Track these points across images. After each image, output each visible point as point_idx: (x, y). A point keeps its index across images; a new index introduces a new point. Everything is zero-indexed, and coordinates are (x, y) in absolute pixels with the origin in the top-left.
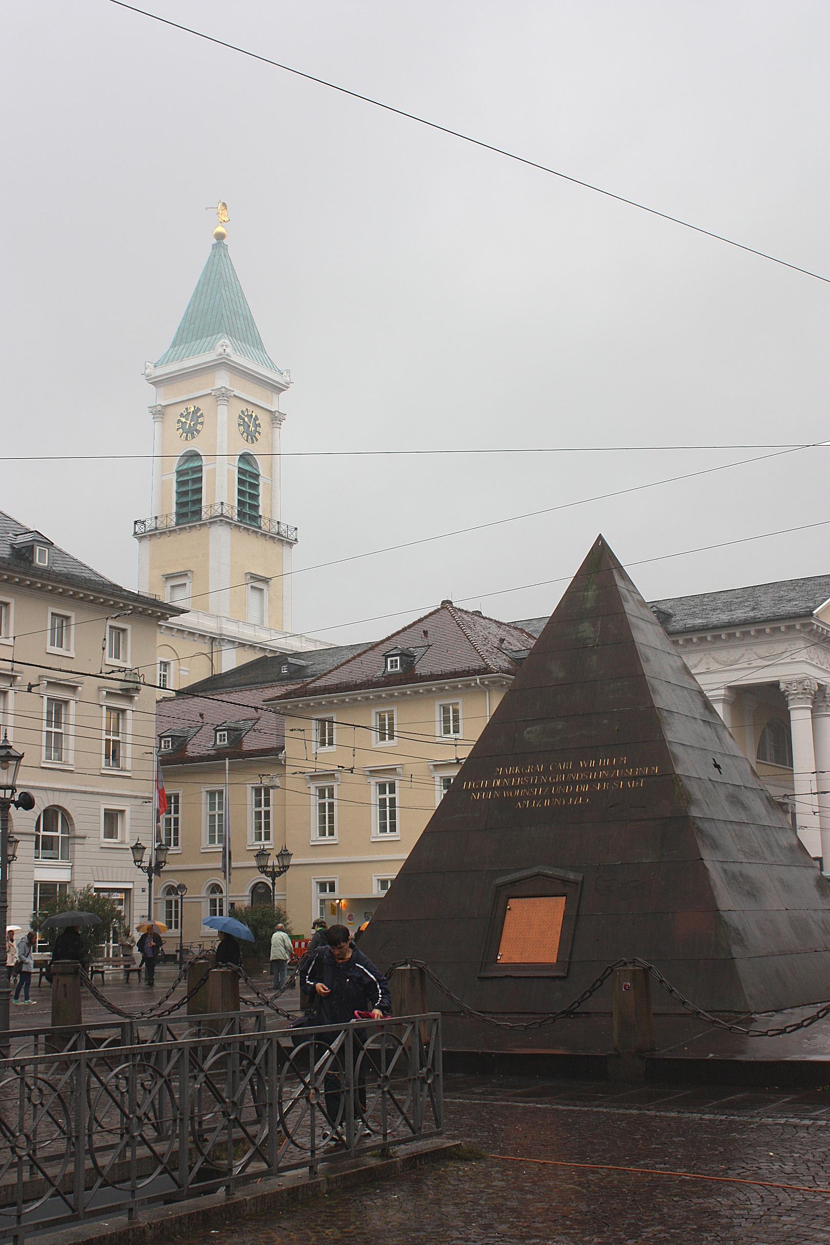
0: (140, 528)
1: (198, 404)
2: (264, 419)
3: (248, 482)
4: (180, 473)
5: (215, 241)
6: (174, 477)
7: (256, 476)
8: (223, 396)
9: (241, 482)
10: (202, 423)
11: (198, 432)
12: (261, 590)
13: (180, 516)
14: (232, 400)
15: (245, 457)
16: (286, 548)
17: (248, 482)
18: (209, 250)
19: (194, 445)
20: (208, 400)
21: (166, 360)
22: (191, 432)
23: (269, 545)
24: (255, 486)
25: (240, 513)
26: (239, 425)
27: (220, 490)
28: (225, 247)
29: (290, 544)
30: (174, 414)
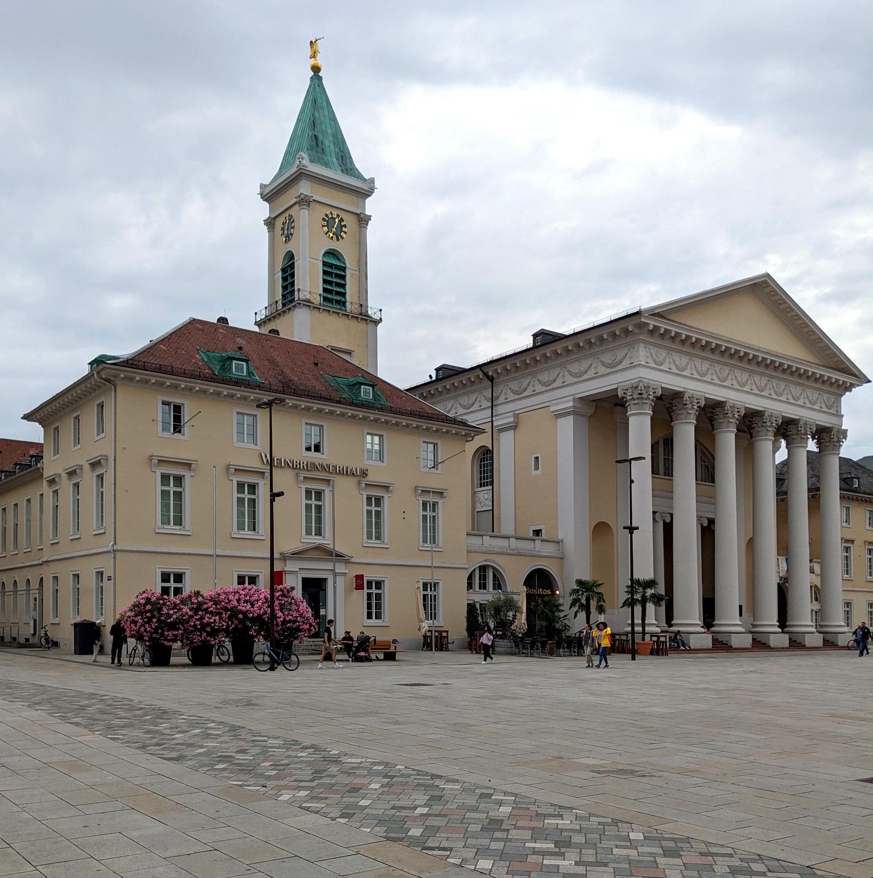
1: (291, 212)
2: (349, 220)
3: (335, 274)
7: (344, 269)
8: (304, 202)
10: (293, 228)
14: (317, 206)
15: (330, 253)
16: (371, 326)
17: (335, 274)
18: (308, 83)
19: (291, 246)
22: (288, 237)
23: (353, 323)
24: (343, 277)
25: (325, 299)
26: (323, 226)
28: (320, 78)
29: (377, 322)
30: (279, 223)
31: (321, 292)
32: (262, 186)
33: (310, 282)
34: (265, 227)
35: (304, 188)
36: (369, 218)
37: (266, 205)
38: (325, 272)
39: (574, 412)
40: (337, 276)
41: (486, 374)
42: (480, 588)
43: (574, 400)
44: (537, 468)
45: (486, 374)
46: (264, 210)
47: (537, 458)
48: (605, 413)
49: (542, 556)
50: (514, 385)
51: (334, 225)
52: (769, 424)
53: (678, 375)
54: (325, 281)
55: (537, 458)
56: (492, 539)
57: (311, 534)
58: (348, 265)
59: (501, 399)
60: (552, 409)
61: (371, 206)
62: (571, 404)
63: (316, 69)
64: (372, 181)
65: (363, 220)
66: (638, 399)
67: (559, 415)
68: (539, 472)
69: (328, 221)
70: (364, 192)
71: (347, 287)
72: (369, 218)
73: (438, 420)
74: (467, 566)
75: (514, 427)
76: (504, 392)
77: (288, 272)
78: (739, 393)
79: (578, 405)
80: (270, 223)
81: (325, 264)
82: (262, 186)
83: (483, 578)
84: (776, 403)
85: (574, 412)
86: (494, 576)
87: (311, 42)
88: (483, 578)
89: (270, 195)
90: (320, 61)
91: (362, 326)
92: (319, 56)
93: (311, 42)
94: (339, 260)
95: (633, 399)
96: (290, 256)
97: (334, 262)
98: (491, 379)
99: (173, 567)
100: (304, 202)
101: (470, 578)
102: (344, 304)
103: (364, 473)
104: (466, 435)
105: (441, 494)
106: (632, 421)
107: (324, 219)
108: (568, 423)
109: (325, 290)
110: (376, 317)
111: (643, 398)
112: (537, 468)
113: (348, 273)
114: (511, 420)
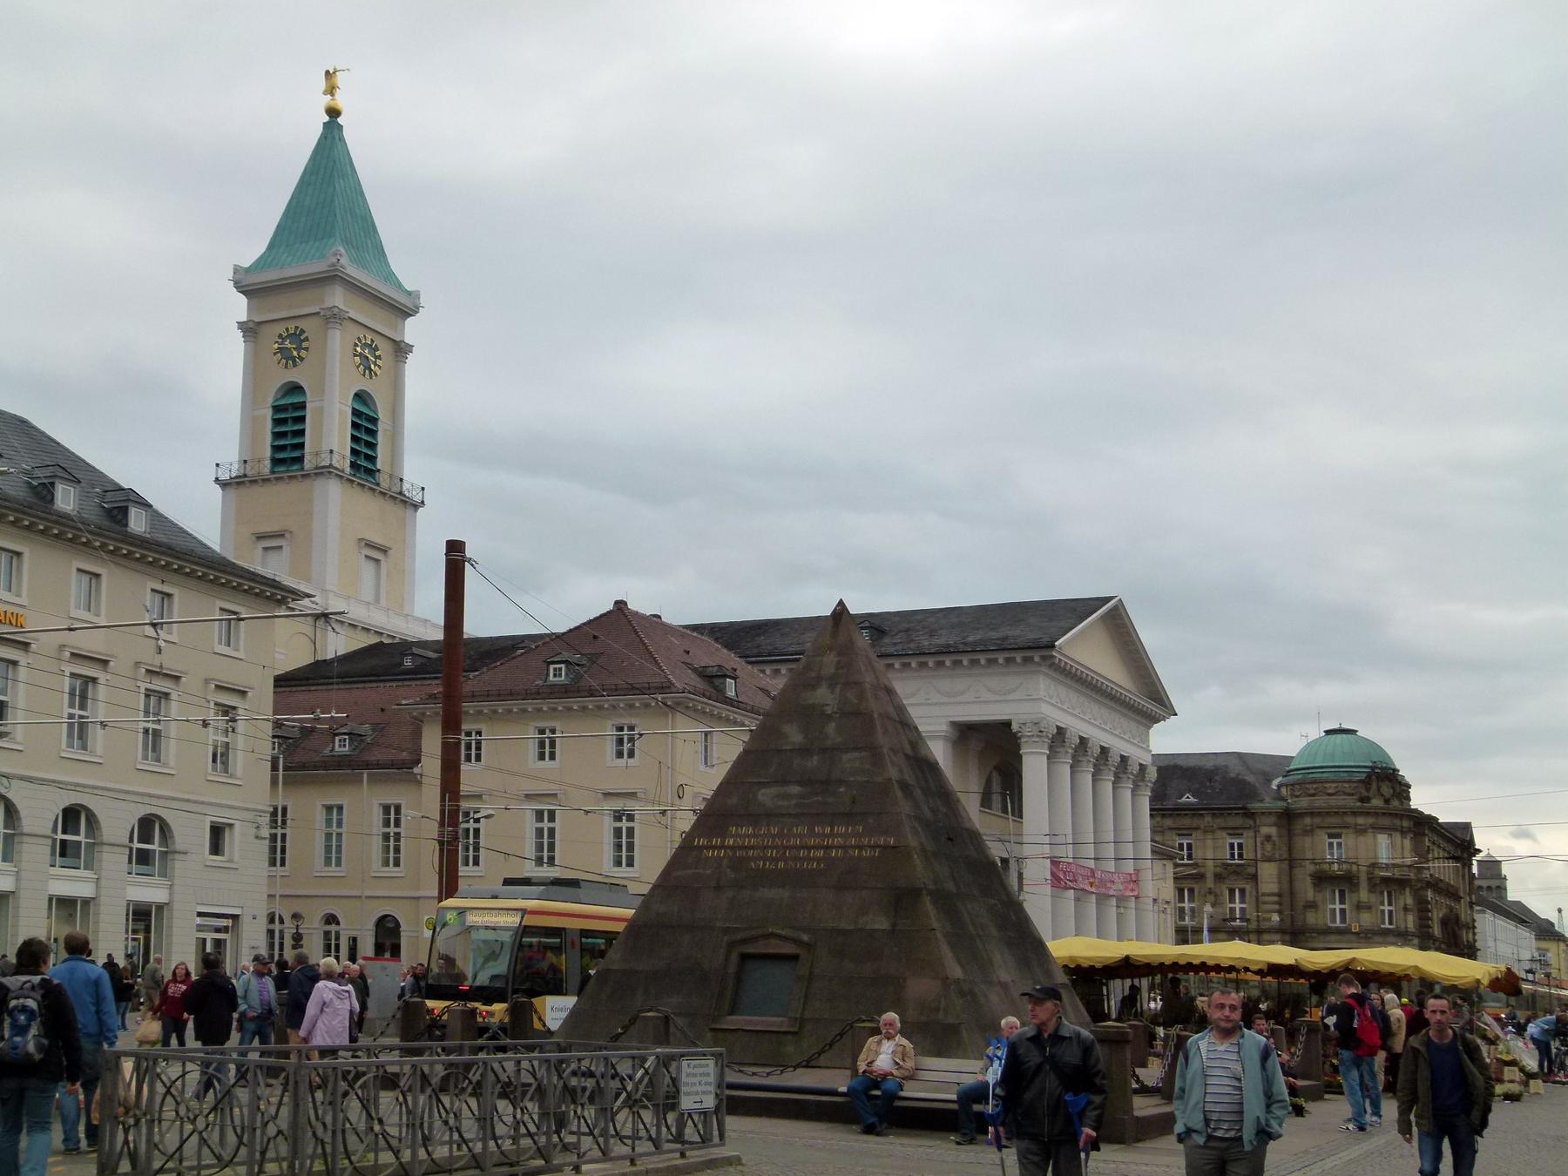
0: (225, 476)
1: (302, 324)
3: (364, 426)
4: (276, 409)
5: (327, 119)
6: (269, 412)
7: (374, 421)
9: (355, 425)
10: (306, 349)
11: (302, 359)
12: (377, 561)
13: (276, 462)
14: (347, 324)
16: (410, 511)
17: (364, 426)
18: (320, 129)
19: (294, 376)
20: (314, 321)
21: (261, 264)
23: (389, 506)
24: (373, 433)
25: (353, 465)
27: (330, 435)
29: (415, 506)
32: (237, 269)
34: (240, 334)
36: (409, 348)
37: (242, 300)
39: (946, 738)
46: (240, 307)
61: (412, 330)
63: (333, 113)
65: (401, 350)
70: (403, 310)
71: (379, 448)
72: (409, 348)
80: (250, 330)
82: (237, 269)
85: (946, 738)
87: (327, 72)
89: (251, 286)
90: (341, 101)
92: (338, 93)
93: (327, 72)
100: (333, 318)
110: (418, 499)
113: (381, 427)
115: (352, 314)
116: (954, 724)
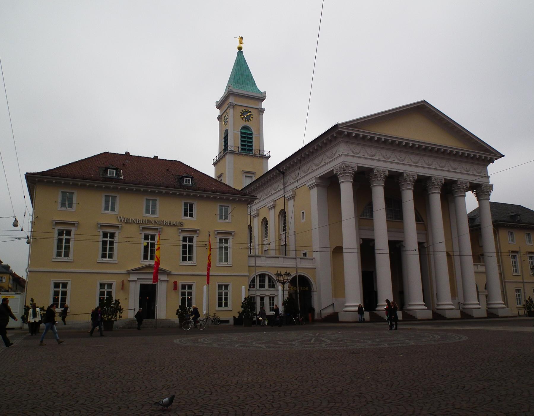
1: (227, 111)
2: (254, 112)
7: (251, 134)
14: (238, 108)
16: (265, 160)
24: (251, 138)
25: (241, 149)
31: (240, 146)
32: (217, 102)
33: (234, 142)
35: (231, 100)
36: (264, 110)
38: (241, 137)
39: (317, 185)
40: (248, 138)
41: (279, 171)
42: (260, 287)
43: (316, 178)
44: (303, 219)
45: (279, 171)
47: (303, 213)
48: (330, 183)
49: (301, 267)
50: (293, 175)
51: (247, 116)
52: (436, 184)
53: (369, 159)
54: (242, 141)
55: (303, 213)
56: (285, 259)
57: (147, 259)
58: (253, 133)
59: (288, 184)
60: (307, 185)
61: (264, 105)
62: (314, 181)
64: (265, 93)
65: (261, 111)
66: (343, 173)
67: (311, 188)
68: (304, 220)
69: (243, 113)
72: (264, 110)
73: (234, 194)
74: (248, 275)
75: (293, 197)
76: (290, 179)
77: (225, 139)
78: (412, 167)
79: (319, 181)
80: (219, 118)
81: (242, 133)
82: (217, 102)
83: (262, 281)
84: (439, 171)
85: (317, 185)
86: (269, 278)
88: (262, 281)
89: (219, 106)
91: (260, 160)
94: (249, 130)
95: (340, 174)
96: (227, 131)
97: (246, 132)
98: (283, 173)
99: (61, 279)
101: (253, 281)
102: (251, 150)
103: (181, 224)
104: (246, 201)
105: (230, 234)
106: (342, 186)
107: (241, 113)
108: (314, 192)
109: (241, 145)
111: (346, 173)
112: (303, 219)
113: (254, 136)
114: (291, 193)
115: (236, 103)
116: (321, 178)
